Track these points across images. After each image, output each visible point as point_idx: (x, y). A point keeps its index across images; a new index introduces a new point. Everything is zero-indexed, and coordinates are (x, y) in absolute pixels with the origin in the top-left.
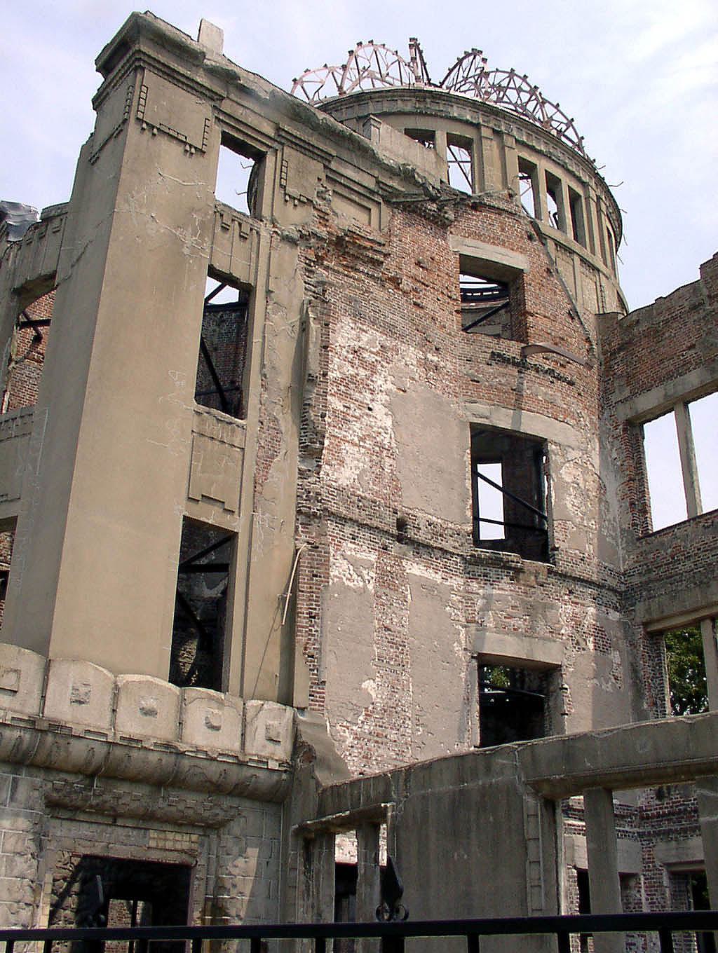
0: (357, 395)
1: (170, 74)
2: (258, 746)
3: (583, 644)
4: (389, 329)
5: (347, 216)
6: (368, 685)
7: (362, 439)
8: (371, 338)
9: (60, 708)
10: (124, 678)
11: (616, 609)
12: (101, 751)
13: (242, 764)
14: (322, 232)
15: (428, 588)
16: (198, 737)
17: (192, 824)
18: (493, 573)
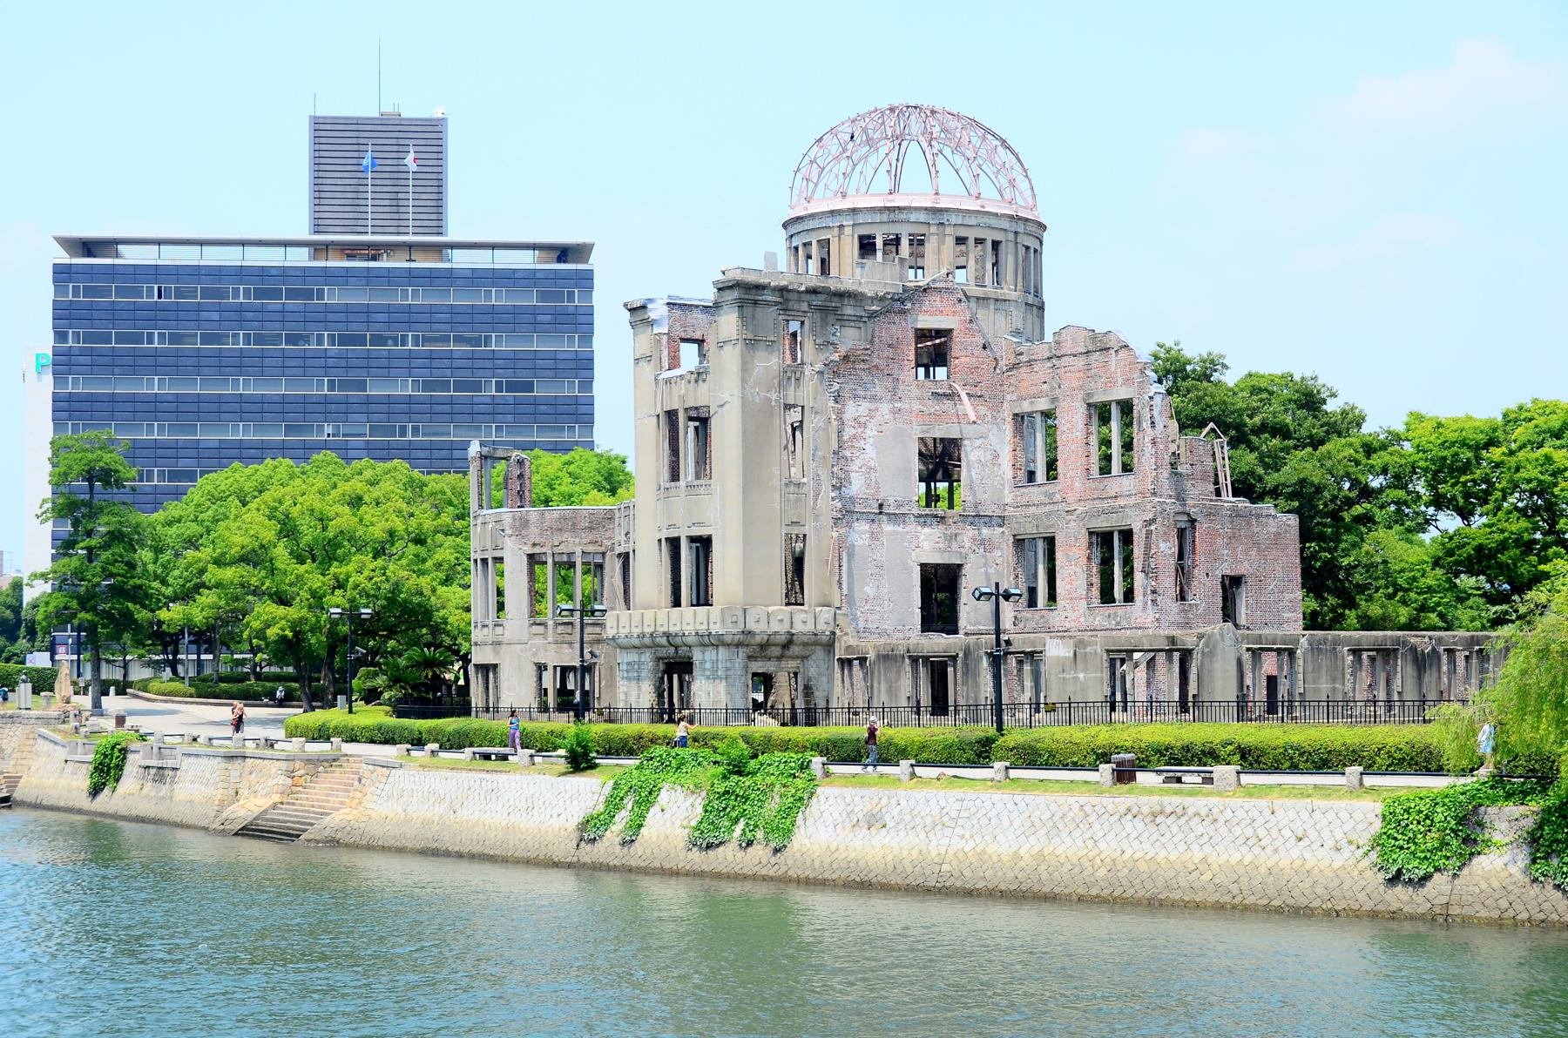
0: (857, 445)
1: (755, 302)
2: (821, 627)
3: (977, 551)
4: (873, 398)
5: (849, 338)
6: (867, 589)
7: (861, 468)
8: (865, 406)
9: (751, 626)
10: (771, 609)
11: (1000, 526)
12: (766, 638)
13: (816, 635)
14: (835, 357)
15: (895, 533)
16: (799, 628)
17: (798, 657)
18: (929, 522)
